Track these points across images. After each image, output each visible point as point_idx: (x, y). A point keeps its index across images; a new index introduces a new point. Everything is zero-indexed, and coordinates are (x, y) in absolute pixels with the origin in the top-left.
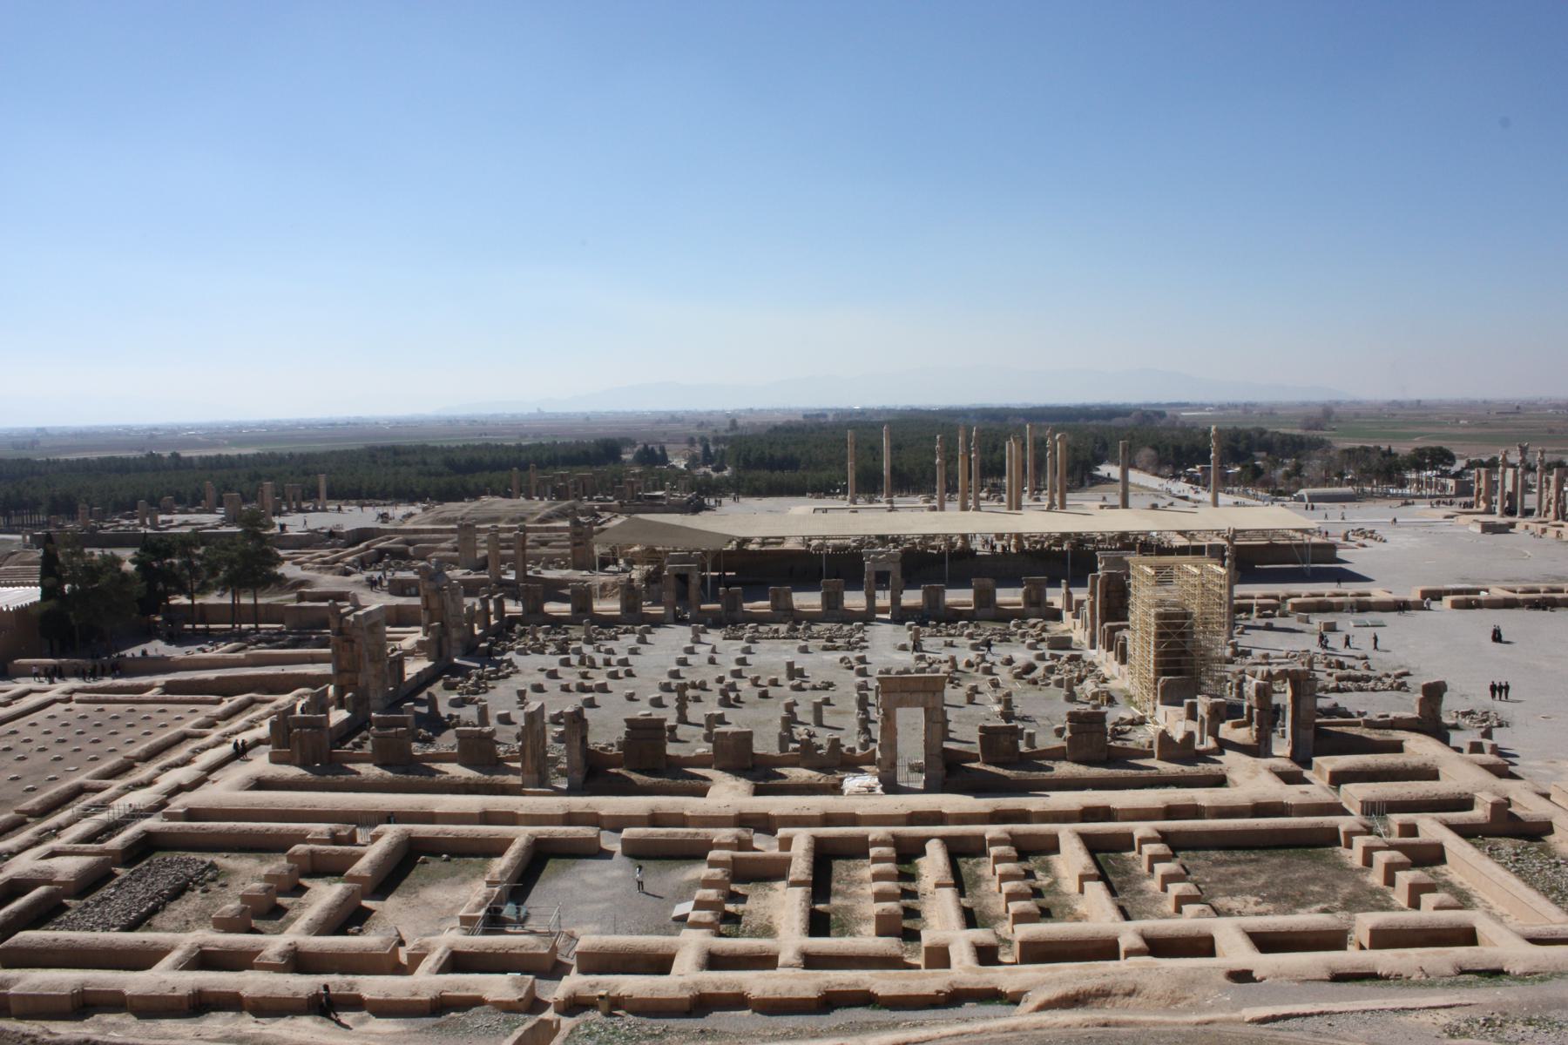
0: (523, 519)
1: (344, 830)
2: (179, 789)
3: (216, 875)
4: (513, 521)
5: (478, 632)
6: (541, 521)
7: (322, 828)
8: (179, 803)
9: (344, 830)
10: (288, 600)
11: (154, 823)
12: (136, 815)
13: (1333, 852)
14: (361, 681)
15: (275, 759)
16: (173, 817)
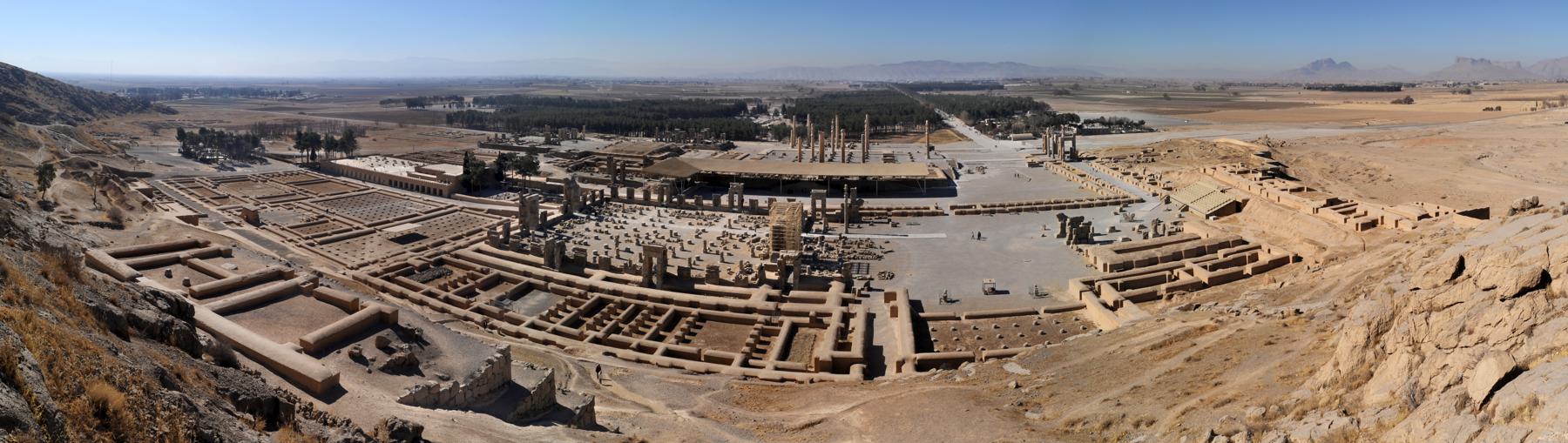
0: (643, 153)
1: (485, 268)
2: (460, 247)
3: (451, 272)
4: (639, 153)
5: (588, 203)
6: (650, 154)
7: (479, 267)
8: (453, 253)
9: (485, 268)
10: (543, 179)
11: (444, 256)
12: (445, 253)
13: (746, 330)
14: (527, 220)
15: (486, 243)
16: (452, 256)
